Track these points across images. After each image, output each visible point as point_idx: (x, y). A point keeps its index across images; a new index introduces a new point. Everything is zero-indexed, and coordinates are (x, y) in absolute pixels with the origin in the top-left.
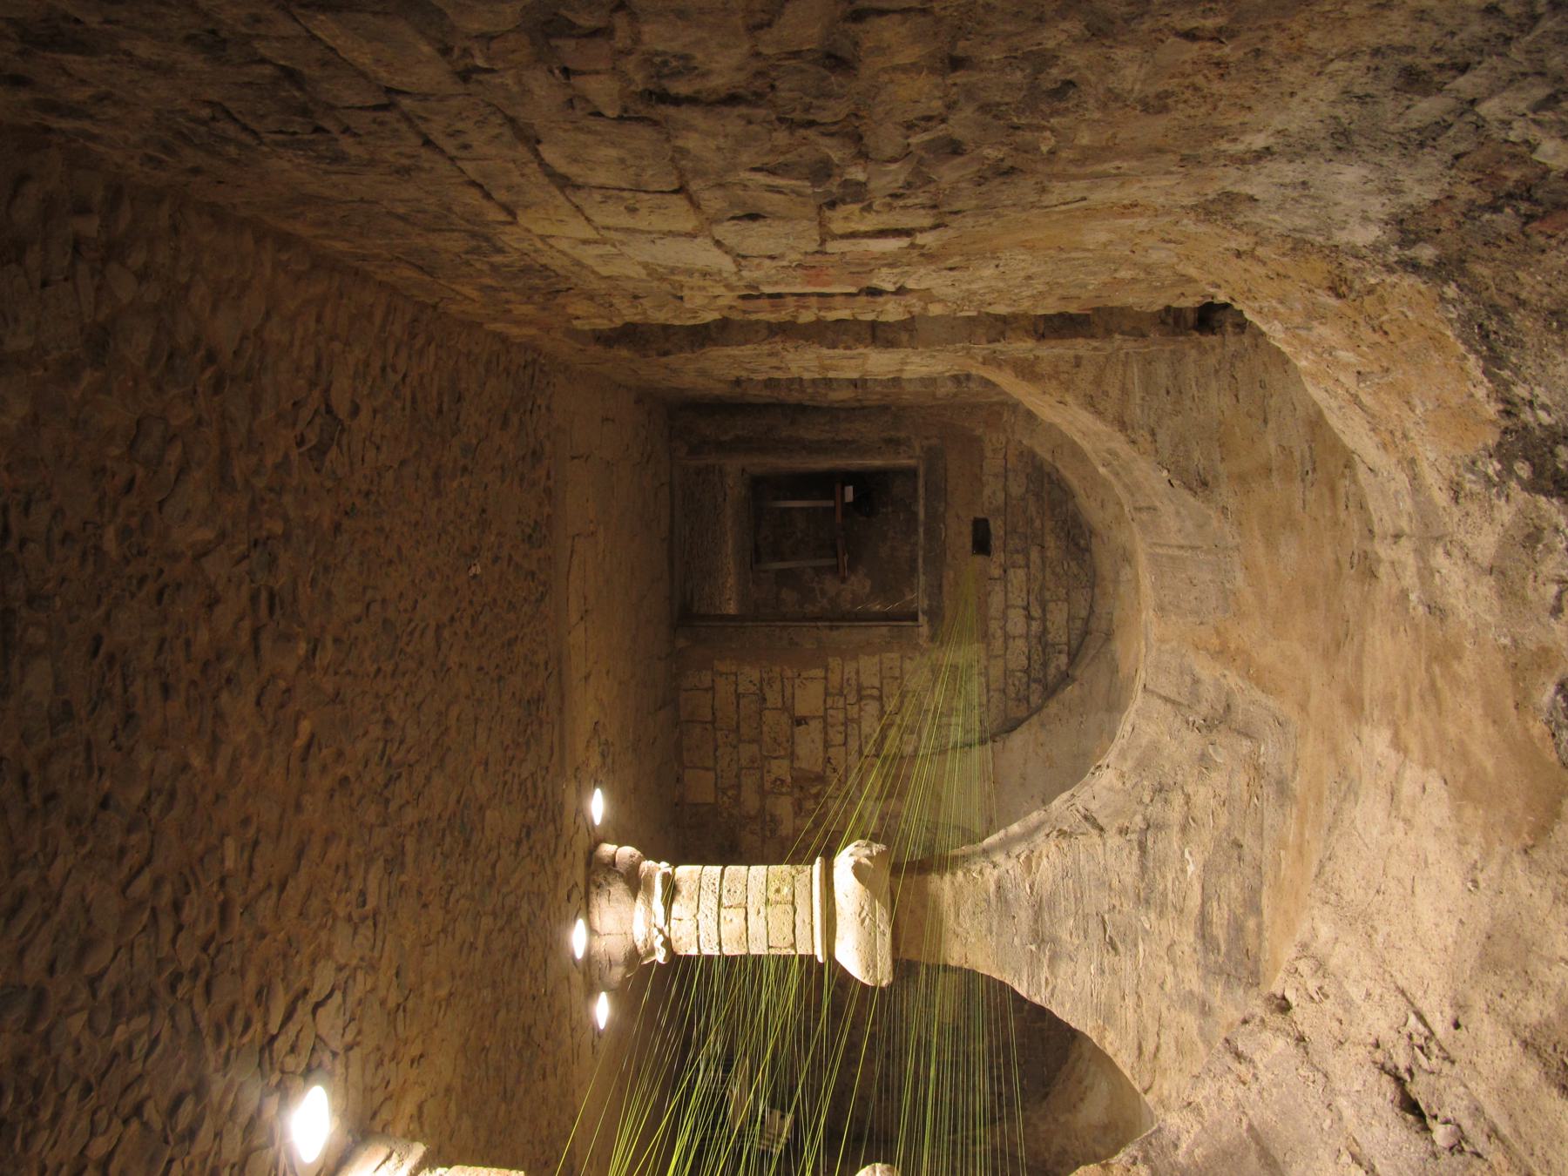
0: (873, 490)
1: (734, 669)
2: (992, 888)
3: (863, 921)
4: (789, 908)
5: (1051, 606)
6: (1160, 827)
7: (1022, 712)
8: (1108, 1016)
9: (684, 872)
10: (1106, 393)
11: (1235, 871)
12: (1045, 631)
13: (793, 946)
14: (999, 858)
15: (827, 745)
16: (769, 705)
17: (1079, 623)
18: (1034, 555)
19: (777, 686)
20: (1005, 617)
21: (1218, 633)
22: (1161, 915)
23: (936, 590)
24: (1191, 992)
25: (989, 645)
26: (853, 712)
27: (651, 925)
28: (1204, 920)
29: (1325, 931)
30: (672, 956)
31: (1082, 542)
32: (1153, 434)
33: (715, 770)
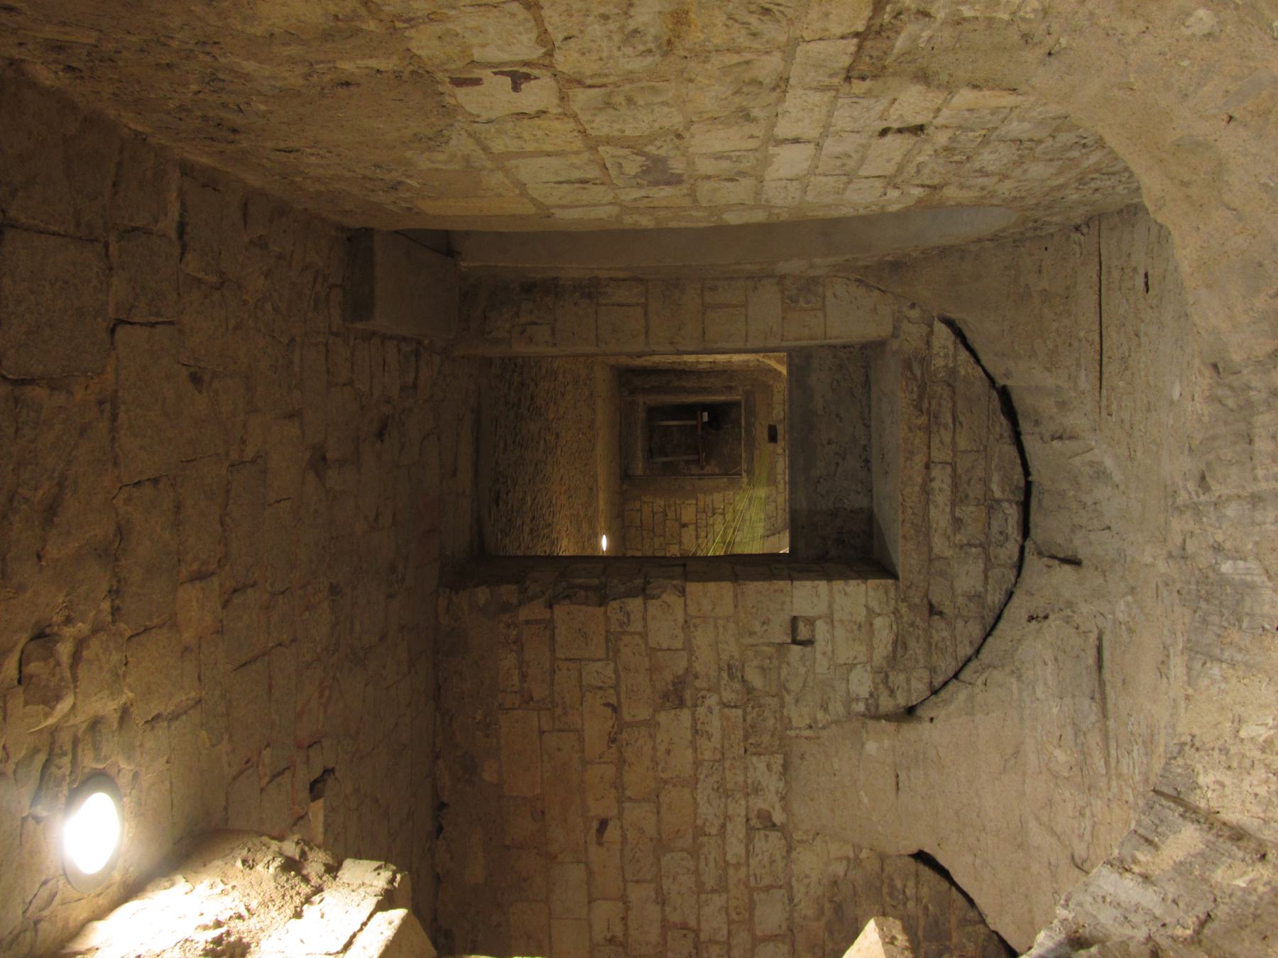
0: (720, 415)
15: (697, 537)
23: (751, 460)
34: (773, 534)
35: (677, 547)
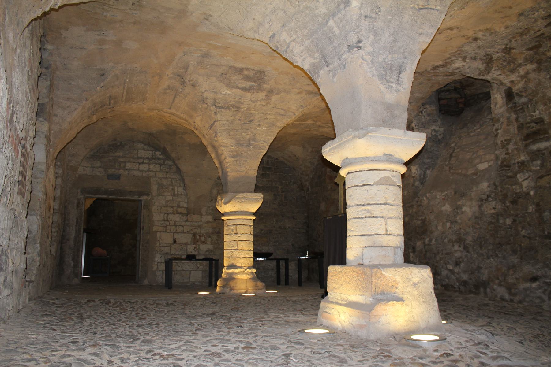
1: (156, 263)
2: (232, 159)
3: (243, 202)
4: (238, 227)
5: (139, 156)
6: (215, 100)
7: (174, 167)
8: (272, 125)
9: (226, 264)
10: (68, 107)
11: (230, 77)
12: (148, 158)
13: (250, 226)
14: (223, 157)
16: (169, 252)
17: (146, 147)
18: (121, 160)
19: (162, 249)
20: (142, 171)
21: (153, 77)
22: (242, 103)
24: (266, 96)
25: (151, 177)
26: (172, 223)
27: (243, 273)
28: (244, 89)
29: (251, 24)
30: (254, 267)
31: (118, 144)
32: (84, 91)
33: (190, 271)
34: (183, 180)
35: (189, 246)
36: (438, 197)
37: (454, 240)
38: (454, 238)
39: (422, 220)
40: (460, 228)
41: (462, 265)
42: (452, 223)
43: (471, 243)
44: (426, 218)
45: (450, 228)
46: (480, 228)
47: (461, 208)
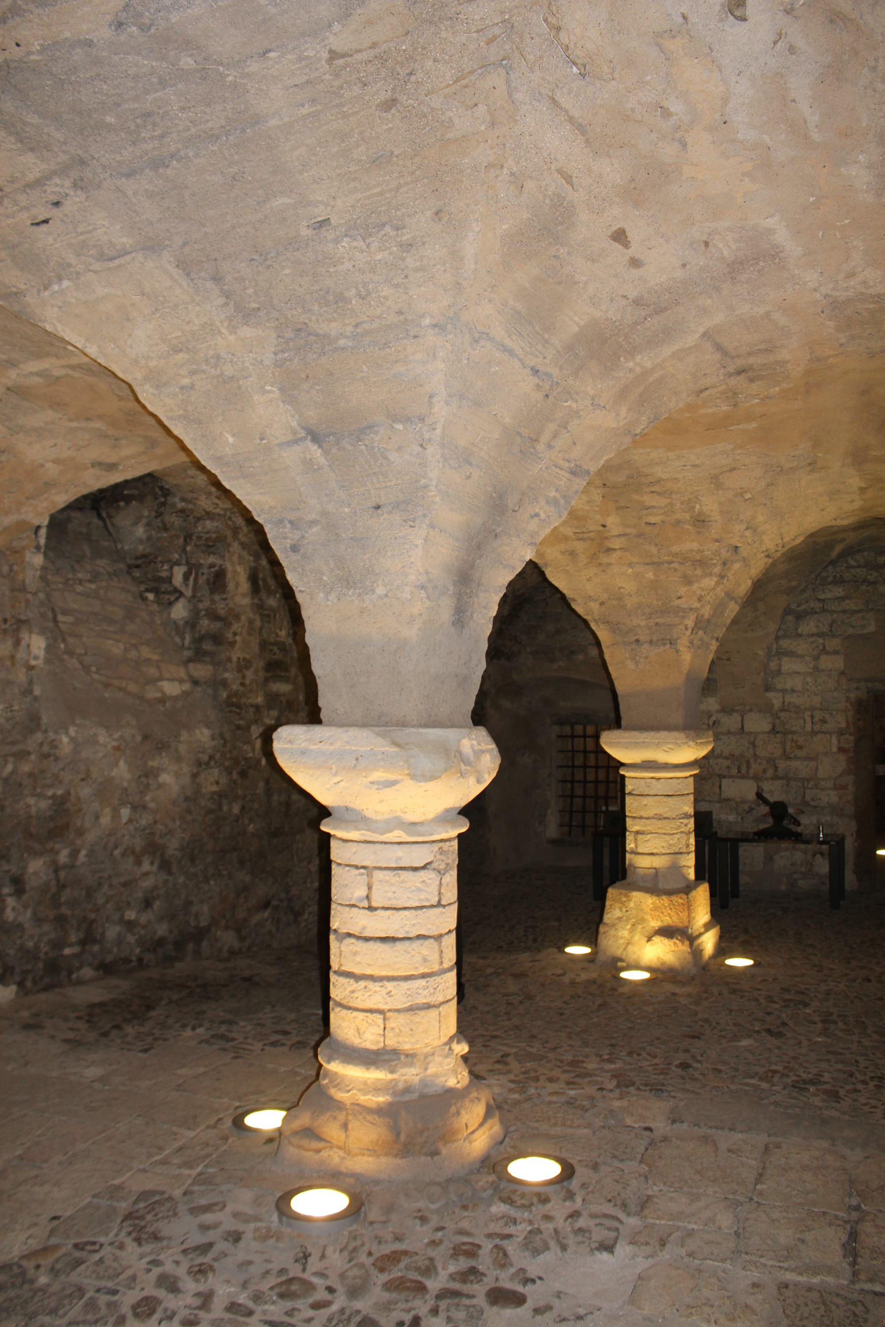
36: (102, 739)
37: (138, 849)
38: (139, 844)
39: (53, 797)
40: (156, 822)
41: (157, 905)
42: (134, 808)
43: (177, 853)
44: (69, 793)
45: (130, 821)
46: (194, 821)
47: (156, 776)
